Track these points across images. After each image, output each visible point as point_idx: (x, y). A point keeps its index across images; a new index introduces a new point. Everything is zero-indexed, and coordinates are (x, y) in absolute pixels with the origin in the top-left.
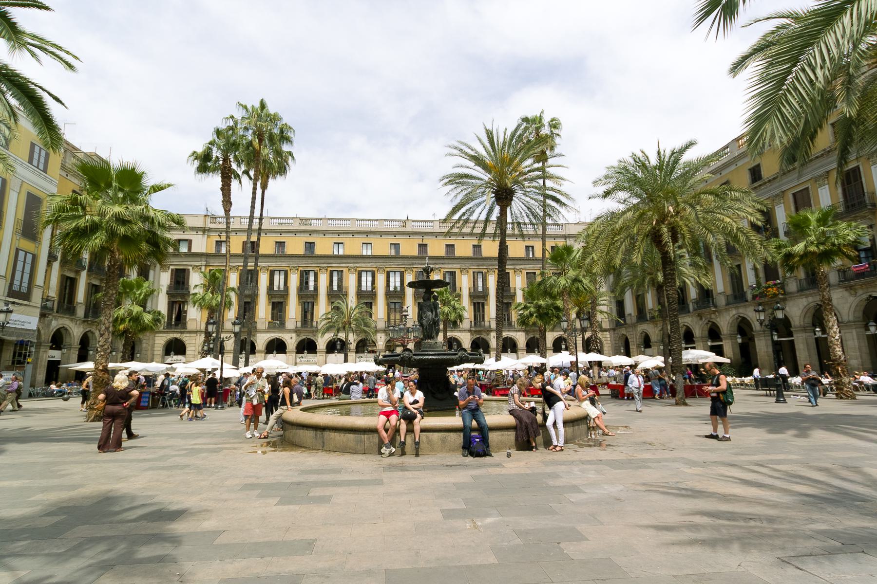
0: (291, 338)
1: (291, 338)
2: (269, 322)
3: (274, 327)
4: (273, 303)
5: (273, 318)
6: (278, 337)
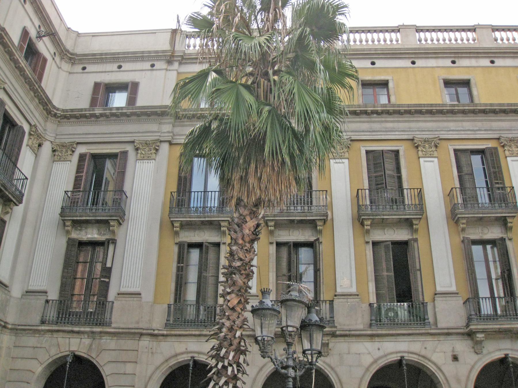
0: (455, 358)
1: (455, 358)
3: (393, 323)
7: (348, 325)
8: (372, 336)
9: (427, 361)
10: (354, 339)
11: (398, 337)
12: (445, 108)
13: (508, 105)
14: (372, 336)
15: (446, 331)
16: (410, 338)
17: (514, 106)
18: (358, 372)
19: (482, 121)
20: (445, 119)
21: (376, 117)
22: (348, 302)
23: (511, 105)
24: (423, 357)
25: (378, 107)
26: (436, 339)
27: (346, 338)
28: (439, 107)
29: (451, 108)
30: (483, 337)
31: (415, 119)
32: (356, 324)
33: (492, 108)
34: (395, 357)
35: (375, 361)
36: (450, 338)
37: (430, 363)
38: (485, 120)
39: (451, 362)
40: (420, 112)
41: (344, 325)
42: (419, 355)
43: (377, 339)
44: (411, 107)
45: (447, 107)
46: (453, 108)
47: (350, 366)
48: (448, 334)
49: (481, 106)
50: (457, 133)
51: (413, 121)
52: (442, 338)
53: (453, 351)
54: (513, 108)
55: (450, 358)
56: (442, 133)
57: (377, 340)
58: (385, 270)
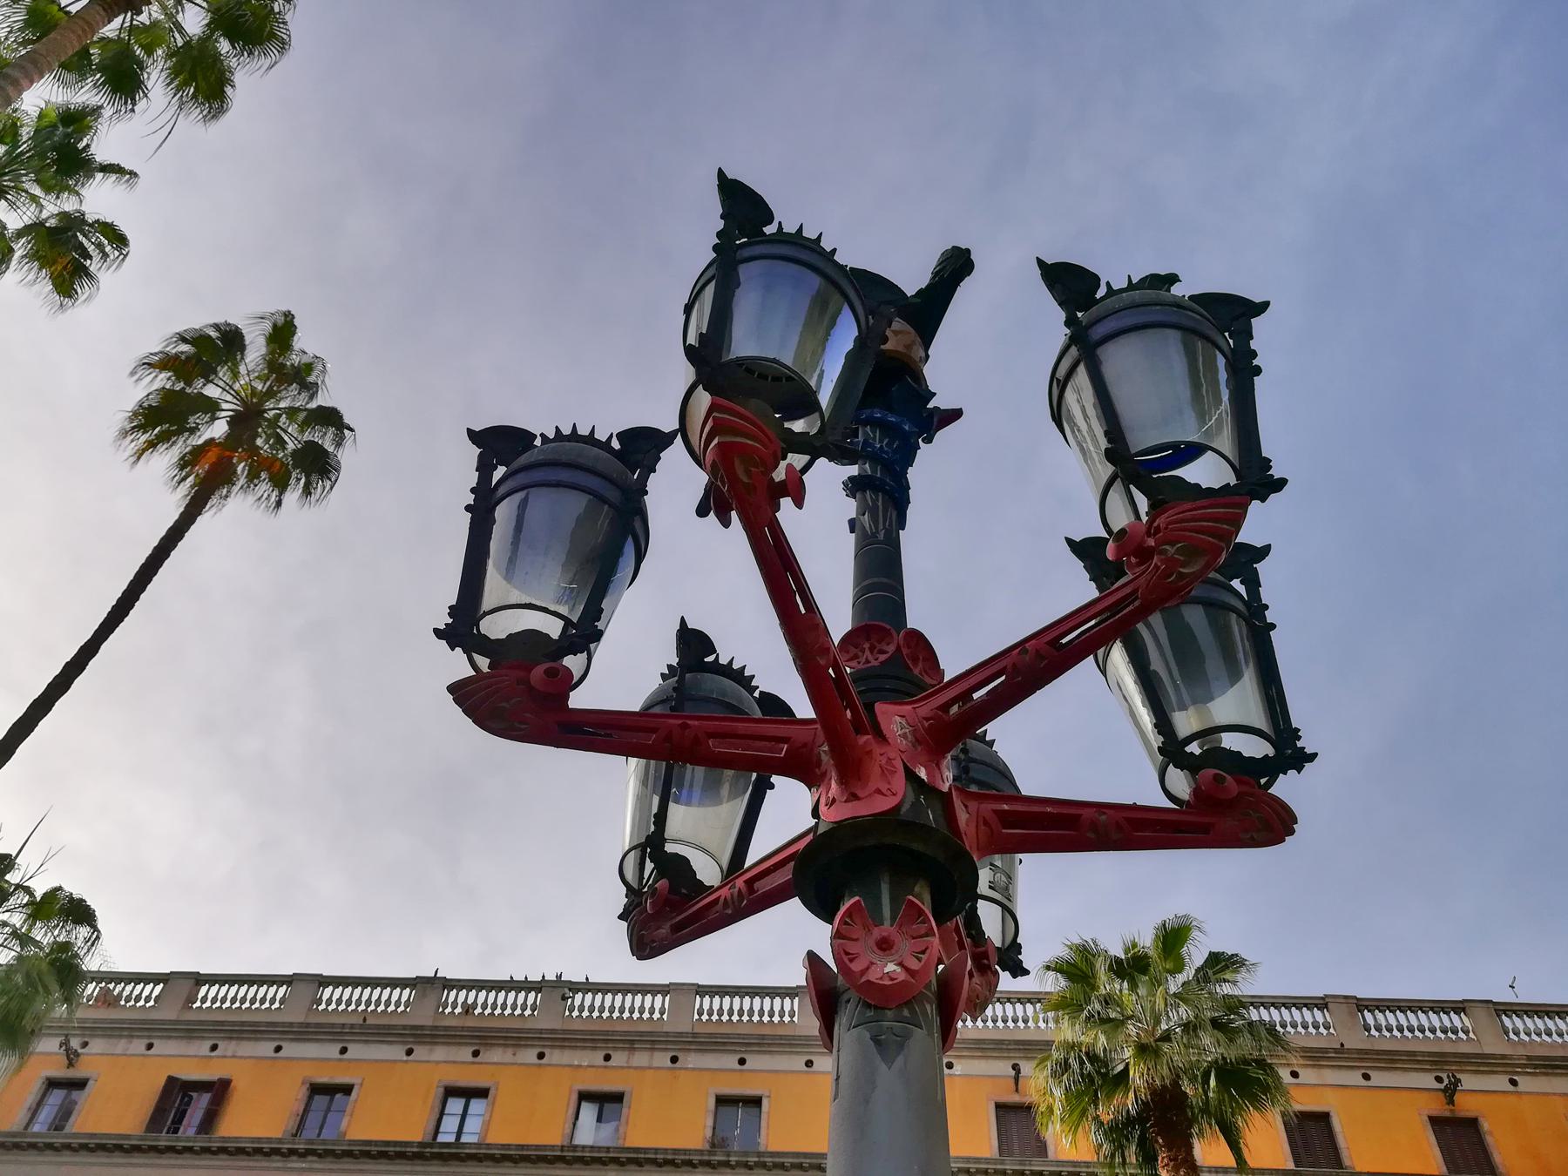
12: (408, 1149)
21: (296, 1161)
25: (299, 1144)
31: (359, 1167)
45: (413, 1147)
49: (469, 1148)
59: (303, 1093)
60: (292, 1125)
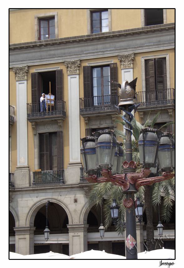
0: (76, 201)
1: (76, 201)
2: (35, 173)
3: (44, 182)
4: (41, 136)
5: (41, 166)
6: (51, 201)
7: (21, 185)
8: (33, 190)
9: (61, 203)
10: (24, 192)
11: (47, 190)
13: (124, 31)
14: (33, 190)
15: (71, 186)
16: (53, 191)
17: (129, 31)
18: (27, 210)
19: (109, 43)
20: (86, 44)
22: (22, 172)
23: (127, 31)
24: (59, 201)
26: (66, 190)
27: (20, 192)
28: (80, 37)
29: (87, 38)
30: (87, 189)
31: (68, 47)
32: (26, 184)
33: (114, 34)
34: (45, 201)
35: (35, 204)
36: (73, 189)
37: (62, 204)
38: (112, 42)
39: (74, 203)
40: (69, 42)
41: (19, 185)
42: (57, 200)
43: (36, 192)
44: (63, 40)
46: (89, 37)
47: (22, 207)
48: (72, 187)
50: (92, 54)
51: (66, 48)
52: (69, 190)
53: (75, 197)
54: (128, 32)
55: (73, 201)
56: (83, 55)
57: (36, 192)
58: (45, 151)
59: (36, 22)
60: (36, 35)
